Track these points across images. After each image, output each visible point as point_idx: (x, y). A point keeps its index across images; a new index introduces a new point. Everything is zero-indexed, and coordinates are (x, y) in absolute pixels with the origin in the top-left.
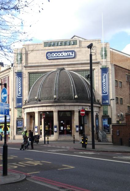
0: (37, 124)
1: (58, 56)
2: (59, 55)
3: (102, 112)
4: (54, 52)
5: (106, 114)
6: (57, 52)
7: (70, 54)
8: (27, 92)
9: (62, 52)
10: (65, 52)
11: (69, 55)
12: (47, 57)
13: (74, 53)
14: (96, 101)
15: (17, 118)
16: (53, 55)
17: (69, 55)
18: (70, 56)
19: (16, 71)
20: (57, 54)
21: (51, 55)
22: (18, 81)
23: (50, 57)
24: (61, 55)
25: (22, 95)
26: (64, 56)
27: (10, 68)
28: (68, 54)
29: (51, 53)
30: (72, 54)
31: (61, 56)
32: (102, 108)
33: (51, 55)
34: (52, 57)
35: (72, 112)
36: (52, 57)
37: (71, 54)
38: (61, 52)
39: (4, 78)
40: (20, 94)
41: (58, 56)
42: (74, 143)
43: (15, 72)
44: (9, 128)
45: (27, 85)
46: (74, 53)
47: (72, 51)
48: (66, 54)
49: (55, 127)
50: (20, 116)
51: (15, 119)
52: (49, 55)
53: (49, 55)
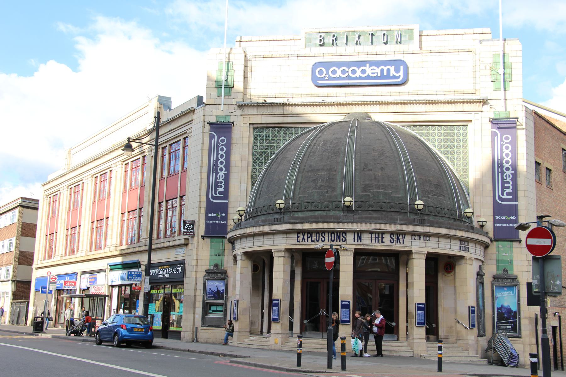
0: (281, 291)
1: (349, 78)
2: (354, 72)
3: (495, 262)
4: (339, 64)
5: (506, 271)
6: (349, 64)
7: (389, 70)
8: (244, 187)
9: (363, 63)
10: (373, 63)
11: (385, 74)
12: (314, 79)
13: (402, 67)
14: (475, 224)
15: (208, 272)
16: (334, 72)
17: (385, 74)
18: (388, 76)
19: (213, 120)
20: (347, 69)
21: (327, 73)
22: (218, 147)
23: (323, 79)
24: (358, 73)
25: (226, 194)
26: (368, 77)
27: (192, 111)
28: (382, 71)
29: (328, 65)
30: (397, 71)
31: (360, 78)
32: (492, 250)
33: (327, 73)
34: (330, 78)
35: (401, 258)
36: (330, 78)
37: (393, 72)
38: (359, 64)
39: (170, 145)
40: (220, 193)
41: (349, 78)
42: (440, 369)
43: (207, 120)
44: (177, 303)
45: (245, 164)
46: (402, 67)
47: (398, 64)
48: (378, 70)
49: (344, 306)
50: (216, 266)
51: (202, 274)
52: (321, 72)
53: (321, 72)
